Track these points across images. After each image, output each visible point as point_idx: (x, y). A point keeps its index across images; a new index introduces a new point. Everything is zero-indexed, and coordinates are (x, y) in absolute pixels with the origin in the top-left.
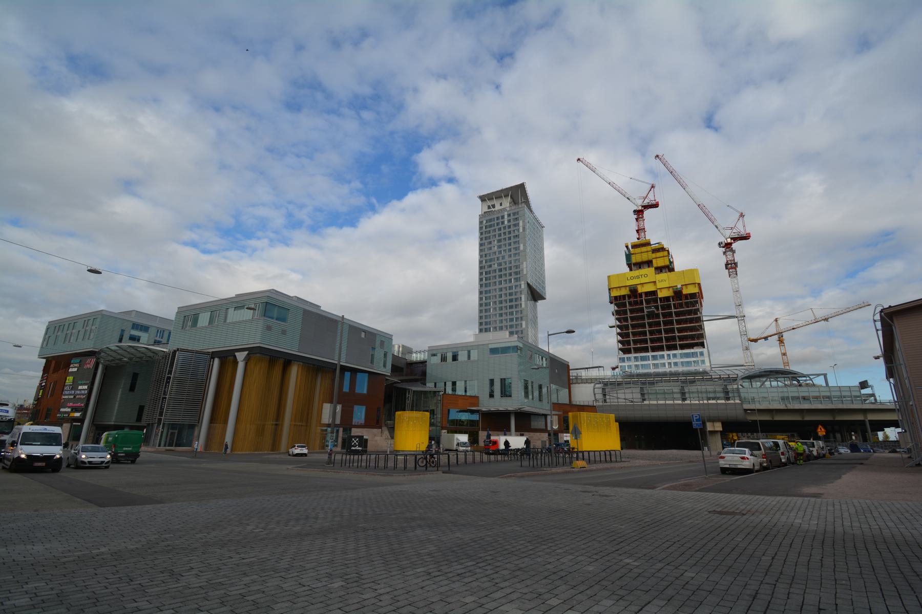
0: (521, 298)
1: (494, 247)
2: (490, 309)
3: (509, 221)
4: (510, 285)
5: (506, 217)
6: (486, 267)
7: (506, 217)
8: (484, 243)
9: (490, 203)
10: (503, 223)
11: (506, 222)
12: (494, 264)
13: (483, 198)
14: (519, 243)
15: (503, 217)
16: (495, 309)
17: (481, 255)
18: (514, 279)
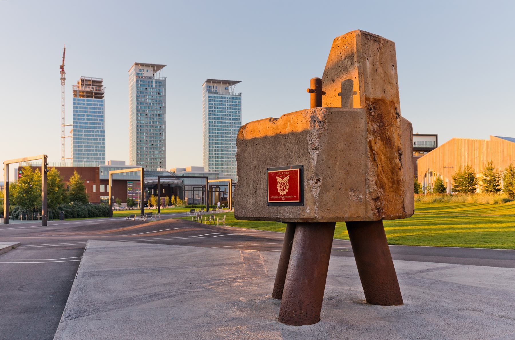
0: (162, 134)
1: (146, 99)
2: (143, 137)
3: (156, 86)
4: (156, 125)
5: (154, 83)
6: (141, 111)
7: (154, 83)
8: (140, 95)
9: (141, 68)
10: (152, 86)
11: (154, 86)
12: (146, 110)
13: (137, 64)
14: (162, 102)
15: (152, 82)
16: (146, 137)
17: (137, 103)
18: (159, 122)
